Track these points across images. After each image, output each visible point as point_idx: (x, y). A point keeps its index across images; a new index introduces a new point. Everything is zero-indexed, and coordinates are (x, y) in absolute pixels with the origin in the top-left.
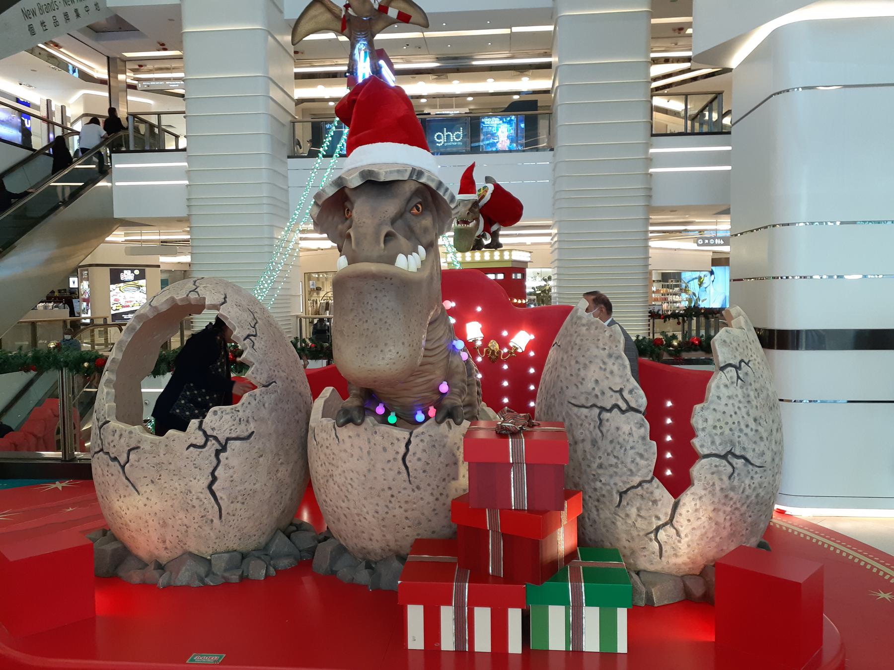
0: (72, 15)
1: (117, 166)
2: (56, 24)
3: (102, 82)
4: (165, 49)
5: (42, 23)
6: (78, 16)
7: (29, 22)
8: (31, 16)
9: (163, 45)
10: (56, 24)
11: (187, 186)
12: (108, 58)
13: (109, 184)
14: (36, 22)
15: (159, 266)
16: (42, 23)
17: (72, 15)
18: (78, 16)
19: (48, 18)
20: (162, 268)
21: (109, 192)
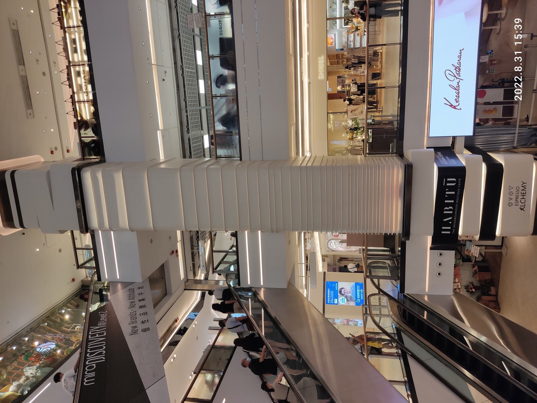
0: (142, 303)
1: (249, 283)
2: (145, 314)
3: (203, 296)
4: (177, 251)
5: (143, 322)
6: (143, 300)
7: (140, 331)
8: (136, 329)
9: (173, 252)
10: (145, 314)
11: (262, 232)
12: (185, 290)
13: (262, 290)
14: (140, 327)
15: (325, 273)
16: (143, 322)
17: (142, 303)
18: (143, 300)
19: (140, 319)
20: (326, 271)
21: (268, 290)
